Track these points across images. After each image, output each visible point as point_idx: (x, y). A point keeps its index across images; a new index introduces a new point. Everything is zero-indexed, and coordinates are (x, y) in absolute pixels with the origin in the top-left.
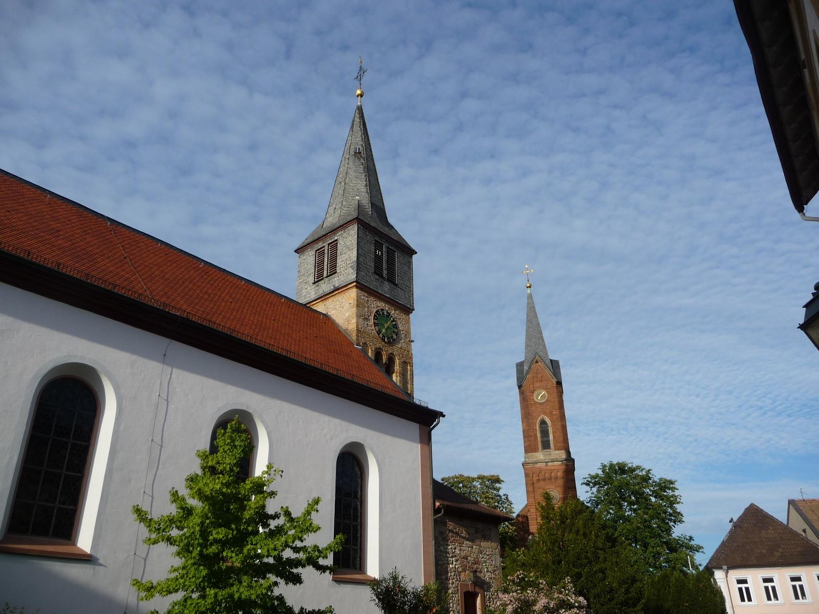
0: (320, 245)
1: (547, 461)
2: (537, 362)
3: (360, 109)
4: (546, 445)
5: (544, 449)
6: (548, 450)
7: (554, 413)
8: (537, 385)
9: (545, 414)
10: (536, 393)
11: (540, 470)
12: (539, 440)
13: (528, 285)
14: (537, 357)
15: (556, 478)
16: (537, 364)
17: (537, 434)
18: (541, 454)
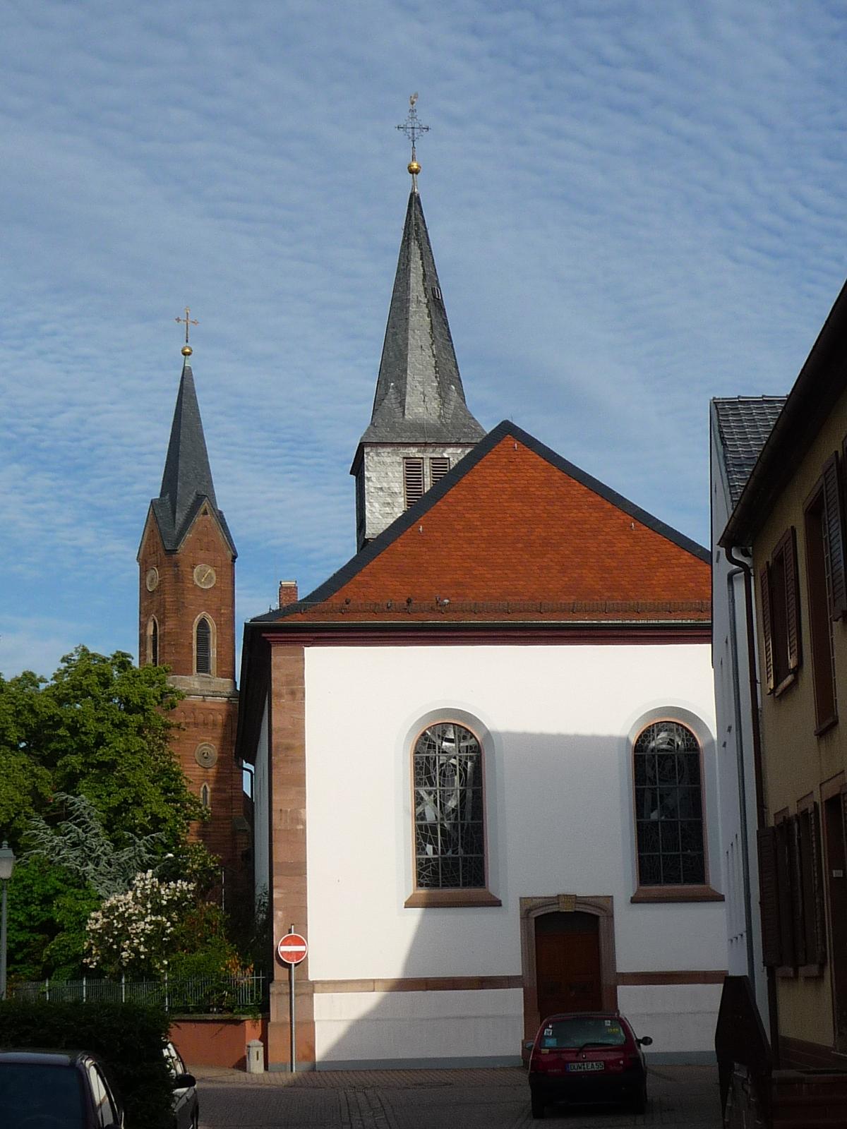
0: (413, 452)
1: (206, 693)
2: (205, 513)
3: (414, 201)
4: (203, 667)
7: (222, 611)
8: (202, 554)
9: (208, 610)
12: (195, 653)
13: (188, 350)
14: (206, 504)
15: (214, 724)
16: (206, 516)
17: (191, 644)
18: (197, 679)
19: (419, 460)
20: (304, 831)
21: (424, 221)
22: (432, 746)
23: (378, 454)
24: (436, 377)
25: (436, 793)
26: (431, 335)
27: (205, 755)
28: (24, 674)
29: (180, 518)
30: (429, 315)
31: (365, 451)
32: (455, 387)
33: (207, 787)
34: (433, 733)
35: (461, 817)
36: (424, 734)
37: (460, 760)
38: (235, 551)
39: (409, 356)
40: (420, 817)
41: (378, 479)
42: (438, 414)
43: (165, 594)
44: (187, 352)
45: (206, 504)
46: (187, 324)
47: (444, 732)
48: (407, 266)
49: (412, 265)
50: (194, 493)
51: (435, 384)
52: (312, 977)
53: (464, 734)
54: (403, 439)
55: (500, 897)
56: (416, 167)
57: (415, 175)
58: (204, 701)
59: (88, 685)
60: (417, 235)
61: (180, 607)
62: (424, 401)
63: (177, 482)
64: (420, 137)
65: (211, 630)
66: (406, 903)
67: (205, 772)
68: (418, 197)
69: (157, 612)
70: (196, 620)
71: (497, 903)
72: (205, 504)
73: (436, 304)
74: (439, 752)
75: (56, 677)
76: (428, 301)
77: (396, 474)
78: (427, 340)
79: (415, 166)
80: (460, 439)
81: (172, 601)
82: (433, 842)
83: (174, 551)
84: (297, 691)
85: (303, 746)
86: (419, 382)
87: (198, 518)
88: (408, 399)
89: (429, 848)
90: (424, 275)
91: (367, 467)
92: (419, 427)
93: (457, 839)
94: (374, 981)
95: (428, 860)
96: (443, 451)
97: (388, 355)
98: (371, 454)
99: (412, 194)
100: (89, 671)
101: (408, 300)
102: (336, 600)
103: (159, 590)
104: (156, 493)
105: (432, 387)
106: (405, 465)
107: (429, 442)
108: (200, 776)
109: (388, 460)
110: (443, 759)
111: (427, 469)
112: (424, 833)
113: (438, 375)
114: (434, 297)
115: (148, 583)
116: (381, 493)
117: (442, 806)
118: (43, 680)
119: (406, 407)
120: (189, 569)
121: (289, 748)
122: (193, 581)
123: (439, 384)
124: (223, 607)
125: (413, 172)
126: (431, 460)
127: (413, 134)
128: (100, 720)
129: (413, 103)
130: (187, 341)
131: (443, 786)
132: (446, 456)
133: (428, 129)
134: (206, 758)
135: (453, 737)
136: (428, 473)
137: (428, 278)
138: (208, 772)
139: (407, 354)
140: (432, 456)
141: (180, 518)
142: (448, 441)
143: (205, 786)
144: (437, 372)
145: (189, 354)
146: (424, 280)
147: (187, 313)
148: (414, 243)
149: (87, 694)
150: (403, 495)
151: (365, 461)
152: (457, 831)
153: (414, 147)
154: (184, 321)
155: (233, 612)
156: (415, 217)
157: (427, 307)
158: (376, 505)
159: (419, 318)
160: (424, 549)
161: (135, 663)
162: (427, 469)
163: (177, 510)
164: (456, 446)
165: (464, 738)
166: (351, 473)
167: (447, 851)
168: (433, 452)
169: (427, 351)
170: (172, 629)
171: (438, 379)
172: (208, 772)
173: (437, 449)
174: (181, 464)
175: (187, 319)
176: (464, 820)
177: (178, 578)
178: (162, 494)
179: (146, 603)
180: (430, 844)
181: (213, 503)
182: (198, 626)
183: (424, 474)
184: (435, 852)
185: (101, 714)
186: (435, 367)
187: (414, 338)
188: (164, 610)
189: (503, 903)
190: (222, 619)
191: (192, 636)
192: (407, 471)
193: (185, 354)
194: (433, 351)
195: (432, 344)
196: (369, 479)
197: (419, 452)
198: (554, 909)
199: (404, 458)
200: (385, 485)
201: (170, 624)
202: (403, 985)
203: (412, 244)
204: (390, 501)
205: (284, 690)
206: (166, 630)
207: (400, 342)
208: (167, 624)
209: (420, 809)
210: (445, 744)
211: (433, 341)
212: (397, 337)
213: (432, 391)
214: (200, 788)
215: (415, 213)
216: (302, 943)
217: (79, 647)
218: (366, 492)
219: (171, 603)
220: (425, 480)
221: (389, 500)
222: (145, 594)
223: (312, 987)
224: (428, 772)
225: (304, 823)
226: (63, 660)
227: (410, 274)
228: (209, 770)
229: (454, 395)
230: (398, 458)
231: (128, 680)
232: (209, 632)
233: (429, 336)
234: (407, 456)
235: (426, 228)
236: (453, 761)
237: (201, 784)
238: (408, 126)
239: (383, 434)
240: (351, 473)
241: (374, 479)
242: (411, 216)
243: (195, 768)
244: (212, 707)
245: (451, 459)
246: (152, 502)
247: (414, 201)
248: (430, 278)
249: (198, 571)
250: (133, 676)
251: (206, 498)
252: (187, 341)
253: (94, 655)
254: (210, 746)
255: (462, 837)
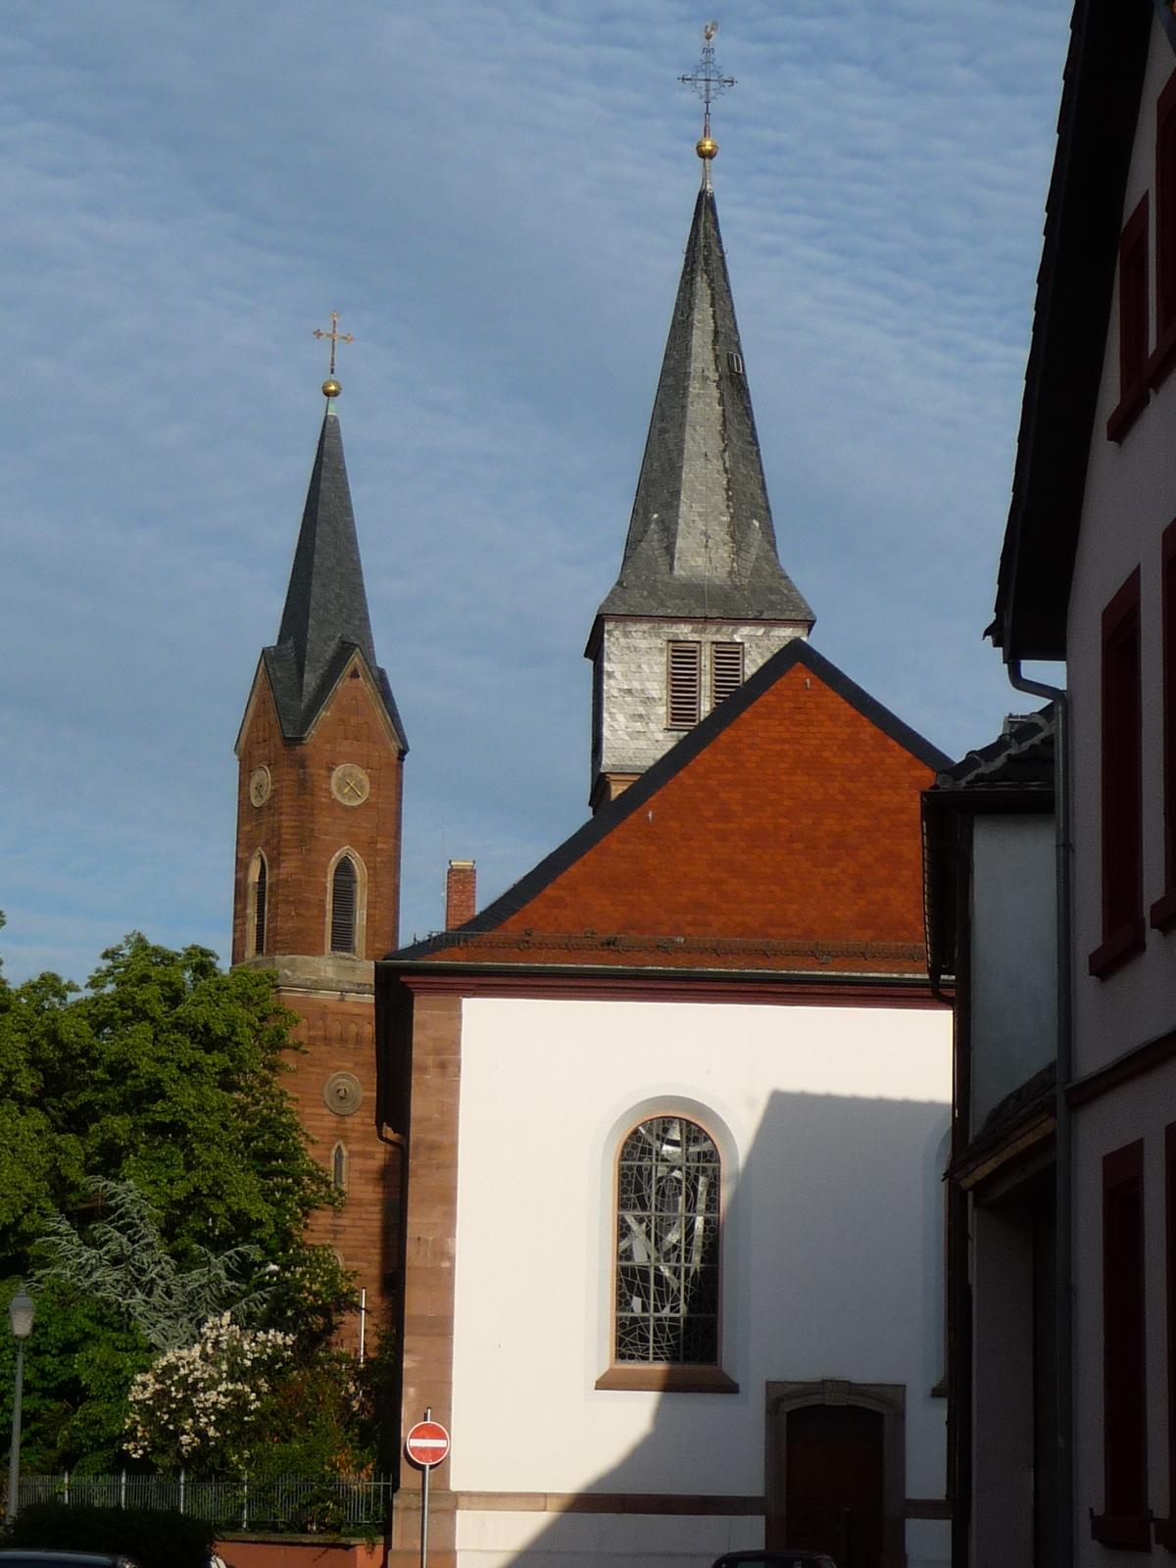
0: (684, 631)
2: (355, 675)
3: (705, 204)
4: (343, 940)
5: (338, 949)
6: (345, 954)
7: (379, 846)
8: (346, 747)
9: (355, 843)
10: (338, 772)
11: (324, 1012)
12: (329, 919)
13: (333, 388)
14: (356, 660)
16: (355, 681)
17: (324, 901)
19: (694, 645)
20: (451, 1271)
21: (719, 241)
22: (646, 1151)
23: (626, 634)
24: (728, 507)
25: (650, 1221)
26: (722, 435)
27: (342, 1093)
28: (43, 977)
29: (311, 680)
30: (721, 402)
31: (606, 628)
32: (760, 522)
33: (343, 1148)
34: (650, 1131)
35: (686, 1258)
36: (636, 1132)
37: (688, 1173)
38: (403, 740)
39: (685, 469)
40: (625, 1255)
41: (625, 675)
42: (727, 569)
43: (282, 814)
44: (332, 391)
45: (356, 660)
46: (334, 340)
47: (666, 1130)
48: (688, 317)
49: (697, 316)
50: (337, 640)
51: (725, 519)
52: (456, 1484)
53: (694, 1134)
54: (670, 611)
55: (737, 1379)
56: (710, 148)
57: (707, 160)
58: (342, 1000)
59: (144, 1002)
60: (707, 264)
61: (305, 838)
62: (706, 547)
63: (308, 617)
64: (718, 96)
65: (359, 878)
66: (597, 1382)
67: (337, 1122)
68: (712, 198)
69: (267, 842)
70: (333, 859)
71: (731, 1388)
72: (356, 659)
73: (734, 384)
74: (657, 1160)
75: (94, 983)
76: (721, 378)
77: (656, 669)
78: (715, 444)
79: (708, 145)
80: (762, 613)
81: (293, 827)
82: (643, 1293)
83: (298, 741)
84: (448, 1063)
85: (453, 1147)
86: (700, 514)
87: (342, 684)
88: (680, 543)
89: (636, 1302)
90: (716, 333)
91: (608, 655)
92: (695, 590)
93: (679, 1290)
94: (545, 1495)
95: (634, 1320)
96: (734, 632)
97: (652, 465)
98: (616, 633)
99: (702, 194)
100: (145, 979)
101: (687, 375)
102: (512, 927)
103: (271, 807)
104: (271, 639)
105: (721, 523)
106: (670, 652)
107: (710, 616)
108: (330, 1129)
109: (643, 644)
110: (662, 1170)
111: (706, 661)
112: (630, 1280)
113: (731, 504)
114: (731, 370)
115: (253, 792)
116: (629, 699)
117: (658, 1240)
118: (72, 987)
119: (677, 556)
120: (323, 772)
121: (434, 1147)
122: (330, 793)
123: (732, 517)
124: (380, 839)
125: (705, 155)
126: (714, 646)
127: (707, 90)
128: (161, 1060)
129: (709, 37)
130: (332, 371)
131: (661, 1211)
132: (738, 640)
133: (732, 82)
134: (342, 1098)
135: (679, 1139)
136: (708, 667)
137: (721, 338)
138: (344, 1123)
139: (681, 467)
140: (715, 640)
141: (311, 680)
142: (743, 614)
143: (339, 1147)
144: (729, 499)
145: (336, 394)
146: (715, 342)
147: (335, 322)
148: (702, 278)
149: (141, 1014)
150: (664, 702)
151: (606, 644)
152: (679, 1278)
153: (707, 113)
154: (329, 335)
155: (397, 848)
156: (706, 235)
157: (718, 387)
158: (621, 718)
159: (704, 405)
160: (653, 848)
161: (224, 964)
162: (706, 661)
163: (307, 668)
164: (755, 625)
165: (696, 1140)
166: (586, 655)
167: (663, 1307)
168: (718, 631)
169: (714, 461)
170: (292, 874)
171: (732, 511)
172: (344, 1123)
173: (725, 629)
174: (316, 590)
175: (334, 332)
176: (690, 1262)
177: (304, 787)
178: (282, 638)
179: (248, 828)
180: (640, 1296)
181: (369, 657)
182: (336, 871)
183: (701, 670)
184: (645, 1308)
185: (162, 1052)
186: (727, 490)
187: (693, 439)
188: (279, 842)
189: (740, 1387)
190: (379, 859)
191: (326, 887)
192: (674, 663)
193: (327, 394)
194: (724, 463)
195: (724, 451)
196: (611, 675)
197: (692, 631)
198: (814, 1400)
199: (669, 641)
200: (636, 685)
201: (289, 867)
202: (586, 1503)
203: (699, 279)
204: (643, 713)
205: (430, 1061)
206: (281, 877)
207: (671, 446)
208: (283, 865)
209: (624, 1244)
210: (666, 1148)
211: (726, 445)
212: (667, 435)
213: (720, 533)
214: (330, 1150)
215: (705, 227)
216: (440, 1435)
217: (132, 935)
218: (605, 696)
219: (293, 831)
220: (703, 678)
221: (641, 710)
222: (247, 812)
223: (455, 1500)
224: (639, 1189)
225: (451, 1259)
226: (105, 956)
227: (692, 330)
228: (347, 1119)
229: (756, 537)
230: (660, 641)
231: (210, 995)
232: (355, 882)
233: (719, 437)
234: (674, 639)
235: (722, 251)
236: (677, 1174)
237: (334, 1144)
238: (700, 77)
239: (636, 600)
240: (586, 655)
241: (618, 675)
242: (698, 232)
243: (323, 1115)
244: (356, 1011)
245: (746, 645)
246: (263, 652)
247: (705, 204)
248: (726, 338)
249: (340, 775)
250: (218, 989)
251: (357, 650)
252: (332, 371)
253: (156, 951)
254: (352, 1079)
255: (686, 1288)
